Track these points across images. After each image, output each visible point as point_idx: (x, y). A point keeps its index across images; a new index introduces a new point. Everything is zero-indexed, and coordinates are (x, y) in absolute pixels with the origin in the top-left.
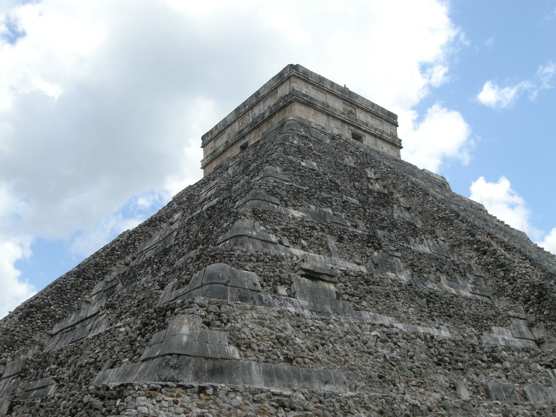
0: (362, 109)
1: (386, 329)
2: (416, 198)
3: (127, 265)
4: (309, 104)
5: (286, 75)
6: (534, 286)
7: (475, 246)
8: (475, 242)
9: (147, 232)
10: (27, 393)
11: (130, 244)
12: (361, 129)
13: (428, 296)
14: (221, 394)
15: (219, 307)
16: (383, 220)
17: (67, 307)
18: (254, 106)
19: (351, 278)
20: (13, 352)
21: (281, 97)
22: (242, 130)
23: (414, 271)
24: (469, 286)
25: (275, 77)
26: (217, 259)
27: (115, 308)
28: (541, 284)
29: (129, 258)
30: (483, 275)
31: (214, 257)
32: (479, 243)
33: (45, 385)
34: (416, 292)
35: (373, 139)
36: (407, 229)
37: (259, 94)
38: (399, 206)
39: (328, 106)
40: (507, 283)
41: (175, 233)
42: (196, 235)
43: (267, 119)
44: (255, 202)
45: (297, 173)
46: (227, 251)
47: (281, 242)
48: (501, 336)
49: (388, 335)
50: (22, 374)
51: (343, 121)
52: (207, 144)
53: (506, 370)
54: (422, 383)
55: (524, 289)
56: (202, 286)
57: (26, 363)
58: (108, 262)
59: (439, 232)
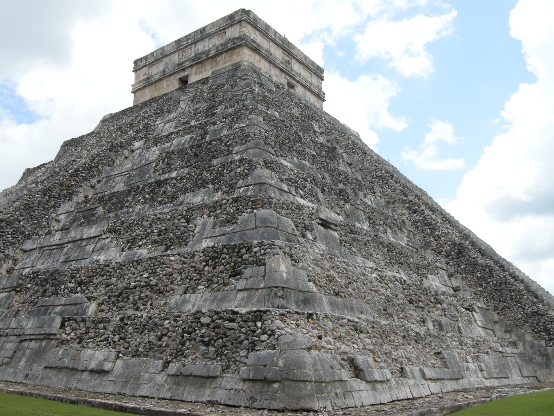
0: (297, 60)
1: (379, 273)
2: (356, 156)
3: (93, 187)
4: (256, 50)
5: (238, 18)
6: (455, 244)
7: (408, 205)
8: (408, 201)
9: (109, 157)
11: (94, 167)
12: (294, 79)
14: (321, 318)
15: (291, 249)
17: (35, 224)
18: (198, 41)
21: (230, 39)
22: (182, 63)
24: (405, 238)
25: (224, 18)
26: (258, 204)
28: (461, 244)
29: (94, 181)
30: (412, 230)
31: (255, 202)
32: (411, 203)
34: (380, 242)
36: (355, 183)
38: (343, 161)
39: (271, 54)
40: (432, 239)
41: (154, 164)
42: (200, 174)
43: (212, 57)
45: (272, 124)
46: (267, 198)
48: (434, 282)
49: (381, 277)
50: (18, 289)
51: (282, 70)
52: (139, 69)
53: (444, 310)
55: (447, 246)
56: (256, 228)
57: (20, 279)
58: (73, 183)
59: (377, 189)
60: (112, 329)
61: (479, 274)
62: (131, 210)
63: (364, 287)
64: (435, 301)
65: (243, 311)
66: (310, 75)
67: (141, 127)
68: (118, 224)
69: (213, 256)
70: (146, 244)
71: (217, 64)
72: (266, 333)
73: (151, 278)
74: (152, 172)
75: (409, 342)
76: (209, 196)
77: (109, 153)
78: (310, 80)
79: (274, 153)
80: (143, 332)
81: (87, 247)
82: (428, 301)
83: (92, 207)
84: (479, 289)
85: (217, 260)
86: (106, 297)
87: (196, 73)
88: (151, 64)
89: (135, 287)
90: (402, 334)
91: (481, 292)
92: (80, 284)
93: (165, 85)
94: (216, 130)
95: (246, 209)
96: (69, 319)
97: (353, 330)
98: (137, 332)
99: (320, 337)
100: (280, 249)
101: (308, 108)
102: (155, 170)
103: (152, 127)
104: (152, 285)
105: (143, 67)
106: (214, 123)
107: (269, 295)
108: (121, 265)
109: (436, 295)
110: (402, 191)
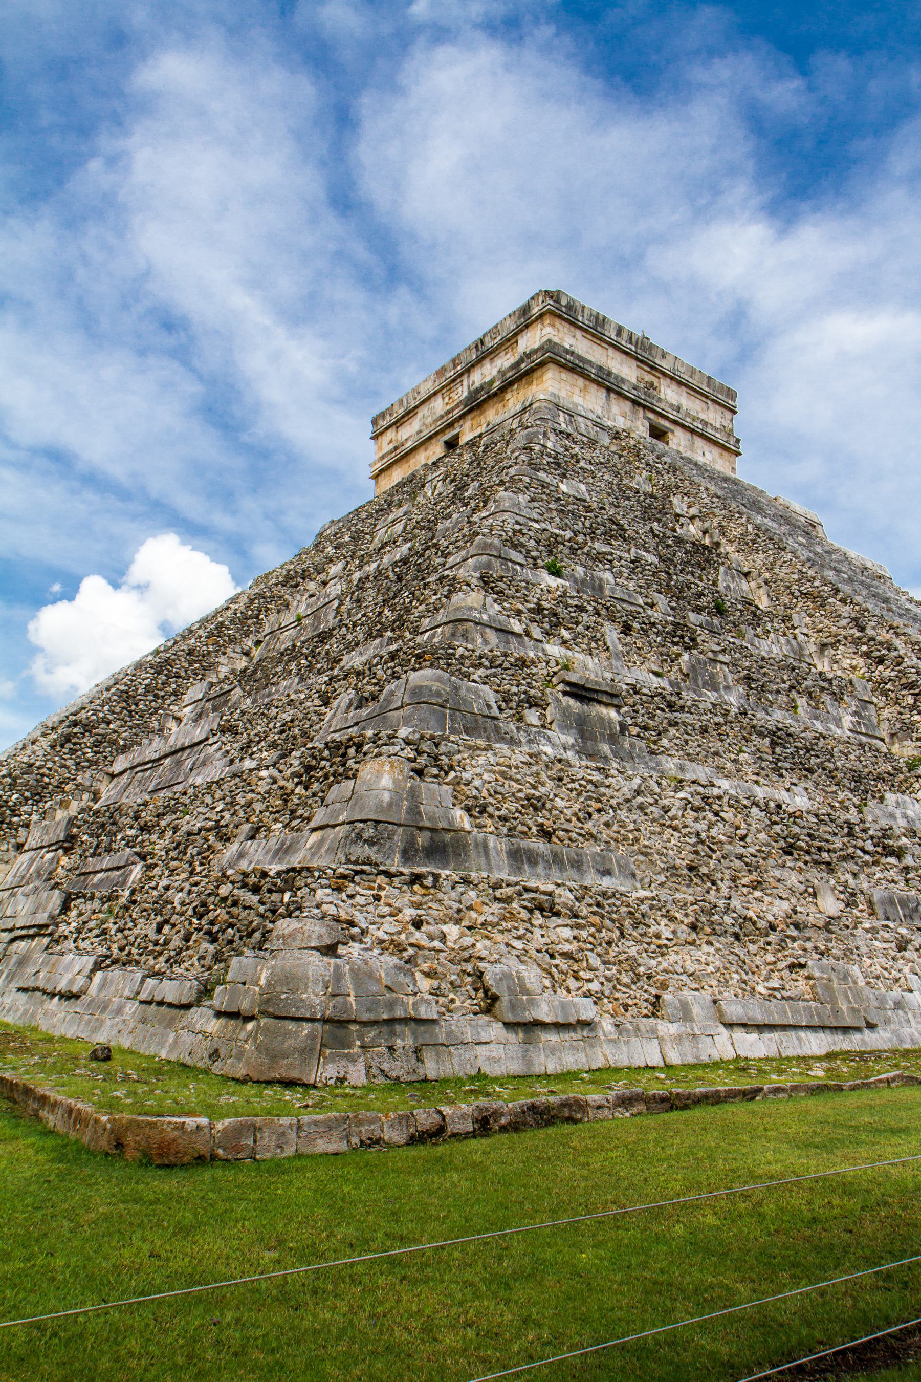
0: (672, 378)
1: (700, 789)
2: (761, 556)
3: (247, 654)
7: (864, 648)
8: (865, 640)
9: (281, 597)
10: (82, 878)
11: (251, 617)
12: (667, 418)
13: (774, 734)
15: (437, 745)
16: (700, 595)
18: (473, 366)
19: (644, 698)
20: (41, 804)
23: (751, 689)
27: (237, 734)
29: (249, 643)
32: (872, 643)
33: (122, 864)
34: (754, 727)
36: (741, 611)
37: (482, 342)
39: (609, 374)
41: (336, 603)
42: (380, 613)
43: (495, 394)
44: (484, 558)
45: (552, 506)
46: (443, 648)
47: (527, 633)
49: (705, 798)
51: (635, 403)
52: (381, 433)
54: (759, 882)
66: (704, 405)
75: (711, 938)
77: (282, 591)
78: (702, 416)
103: (368, 537)
105: (387, 429)
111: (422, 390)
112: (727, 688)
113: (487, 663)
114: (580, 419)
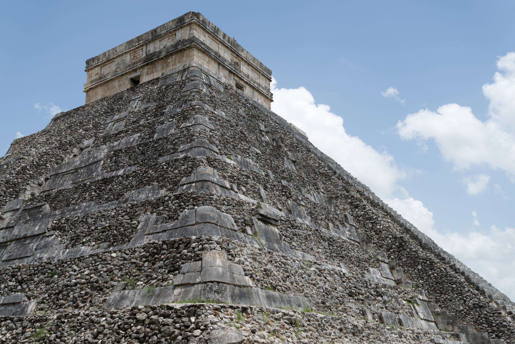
0: (245, 62)
1: (318, 266)
2: (301, 154)
4: (205, 51)
5: (187, 20)
6: (396, 238)
7: (350, 200)
8: (350, 197)
12: (243, 80)
13: (329, 240)
15: (228, 244)
21: (180, 41)
23: (312, 218)
24: (347, 233)
26: (199, 201)
27: (64, 231)
28: (401, 237)
30: (354, 224)
31: (197, 199)
32: (353, 198)
34: (321, 237)
35: (252, 90)
37: (155, 32)
38: (288, 158)
39: (220, 56)
40: (374, 233)
41: (102, 162)
42: (146, 172)
43: (163, 58)
44: (202, 149)
46: (208, 195)
47: (232, 189)
49: (320, 271)
51: (230, 72)
52: (92, 69)
53: (385, 302)
55: (388, 239)
58: (20, 181)
59: (320, 185)
60: (48, 328)
61: (420, 267)
62: (77, 208)
63: (303, 280)
64: (375, 293)
65: (178, 306)
66: (258, 76)
67: (91, 126)
68: (63, 222)
69: (153, 253)
70: (89, 241)
71: (167, 66)
72: (199, 328)
73: (92, 275)
74: (99, 170)
75: (347, 335)
76: (154, 193)
77: (59, 152)
78: (258, 81)
79: (218, 151)
80: (79, 330)
81: (31, 245)
82: (368, 294)
83: (39, 204)
84: (421, 281)
85: (156, 256)
86: (46, 295)
87: (147, 74)
88: (104, 64)
89: (76, 284)
90: (338, 327)
91: (422, 285)
92: (20, 282)
93: (117, 85)
94: (164, 129)
95: (188, 206)
96: (6, 319)
97: (288, 324)
98: (74, 330)
99: (253, 332)
100: (217, 244)
101: (255, 107)
102: (104, 168)
103: (102, 126)
104: (93, 282)
105: (95, 67)
106: (162, 123)
107: (204, 290)
108: (62, 263)
109: (377, 288)
110: (344, 187)
111: (118, 50)
112: (305, 217)
113: (226, 203)
114: (211, 78)
